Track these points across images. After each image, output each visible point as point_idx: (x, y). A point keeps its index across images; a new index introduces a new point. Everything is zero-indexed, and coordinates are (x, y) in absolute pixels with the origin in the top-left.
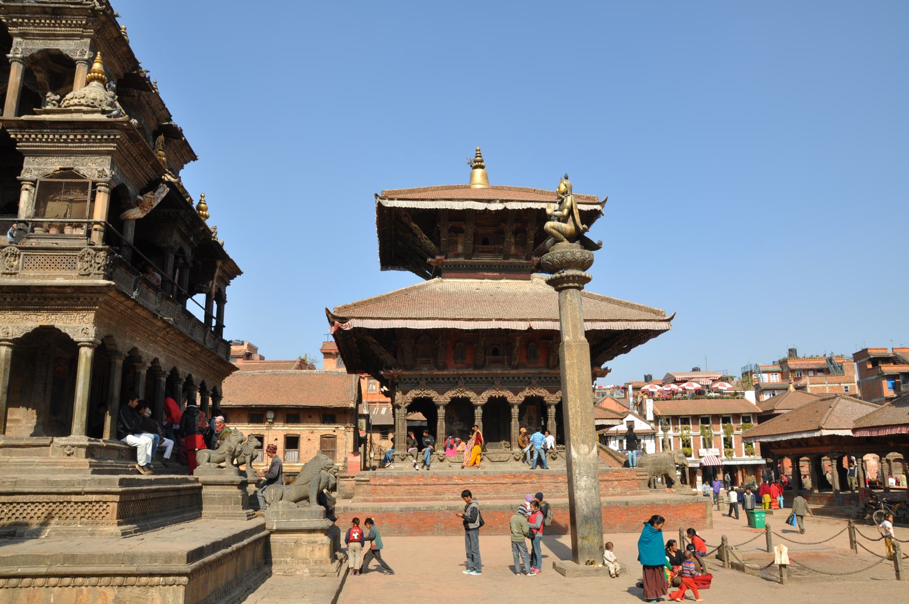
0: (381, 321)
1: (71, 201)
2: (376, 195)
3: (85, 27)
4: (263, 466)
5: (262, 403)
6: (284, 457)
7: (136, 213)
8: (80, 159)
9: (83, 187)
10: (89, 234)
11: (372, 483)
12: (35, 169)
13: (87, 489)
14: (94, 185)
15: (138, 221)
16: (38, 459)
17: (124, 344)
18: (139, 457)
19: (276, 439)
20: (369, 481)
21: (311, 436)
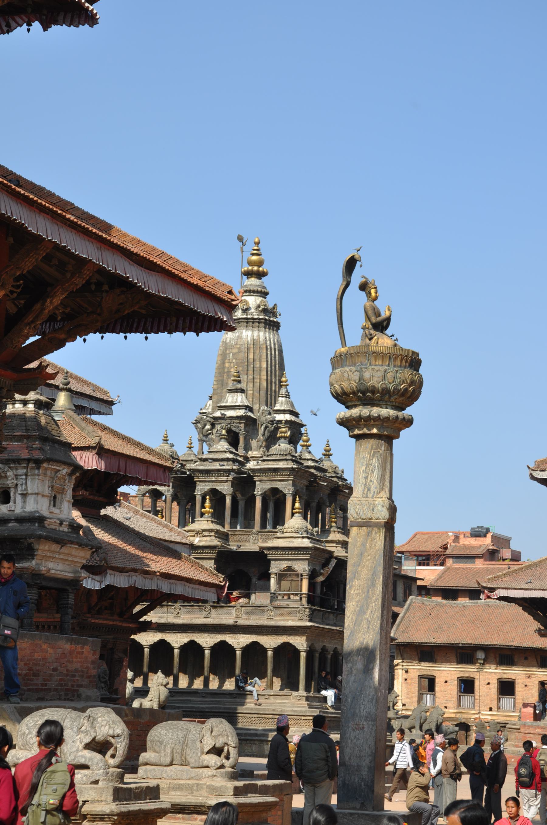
0: (522, 591)
1: (292, 580)
2: (529, 468)
3: (289, 475)
4: (474, 714)
5: (470, 642)
6: (498, 705)
7: (321, 579)
8: (294, 562)
9: (297, 575)
10: (301, 599)
11: (522, 731)
12: (276, 567)
13: (308, 714)
14: (302, 575)
15: (322, 582)
16: (287, 701)
17: (318, 647)
18: (328, 702)
19: (489, 684)
20: (519, 729)
21: (528, 682)
